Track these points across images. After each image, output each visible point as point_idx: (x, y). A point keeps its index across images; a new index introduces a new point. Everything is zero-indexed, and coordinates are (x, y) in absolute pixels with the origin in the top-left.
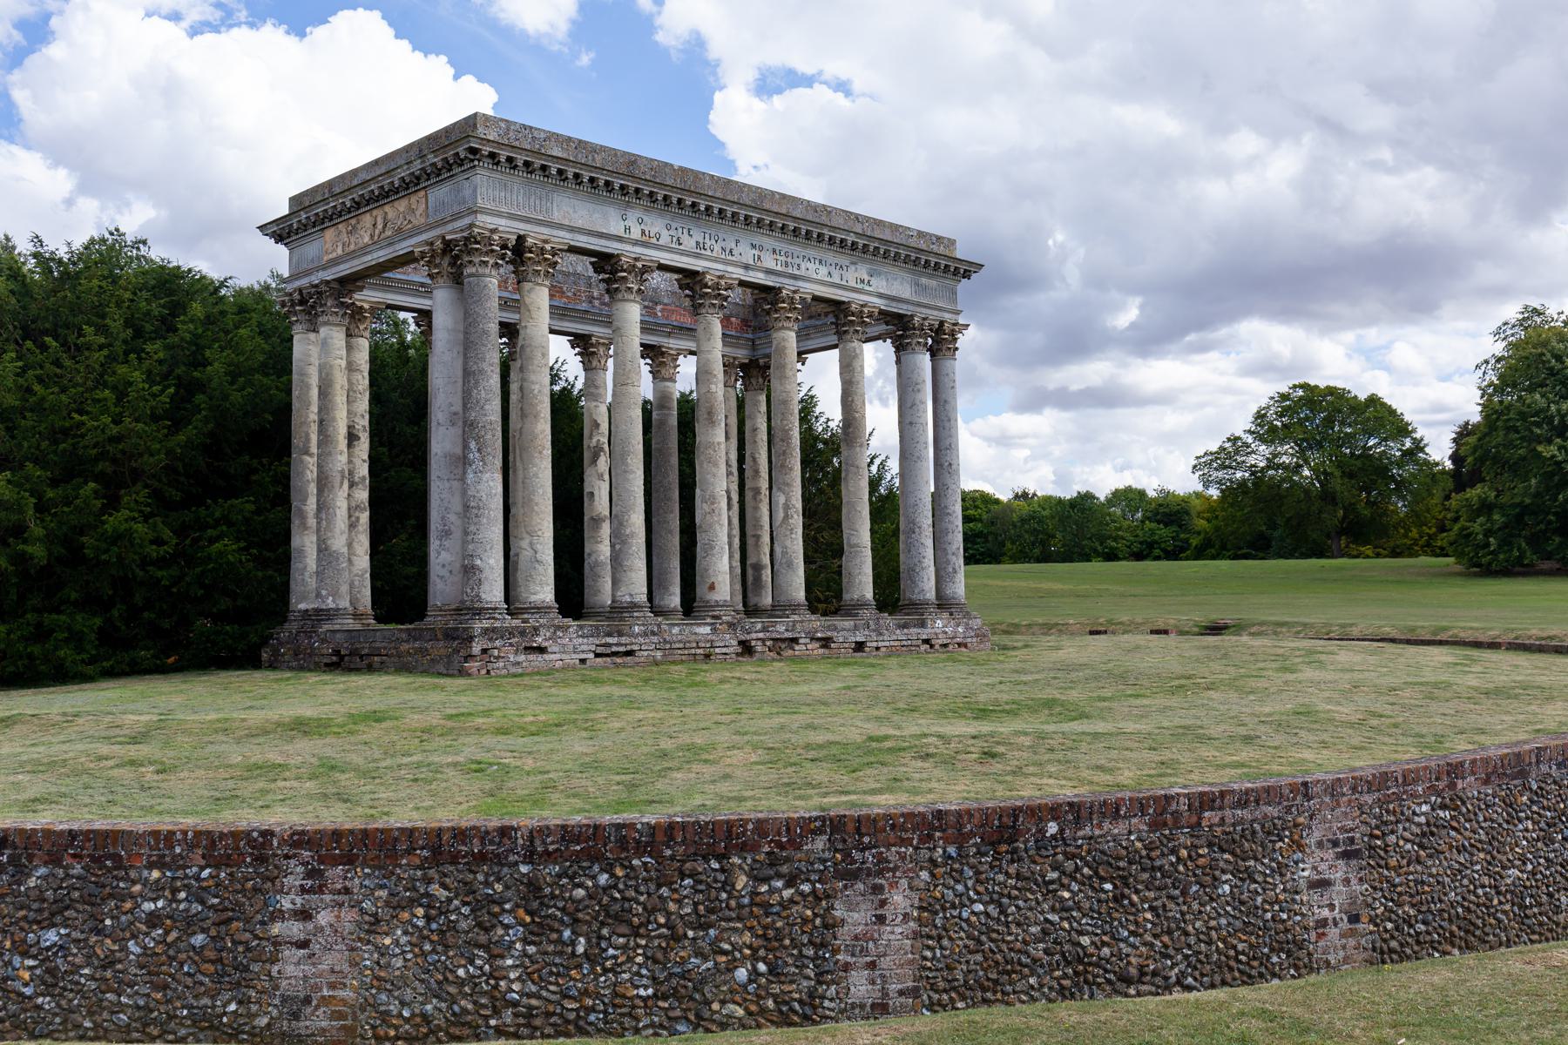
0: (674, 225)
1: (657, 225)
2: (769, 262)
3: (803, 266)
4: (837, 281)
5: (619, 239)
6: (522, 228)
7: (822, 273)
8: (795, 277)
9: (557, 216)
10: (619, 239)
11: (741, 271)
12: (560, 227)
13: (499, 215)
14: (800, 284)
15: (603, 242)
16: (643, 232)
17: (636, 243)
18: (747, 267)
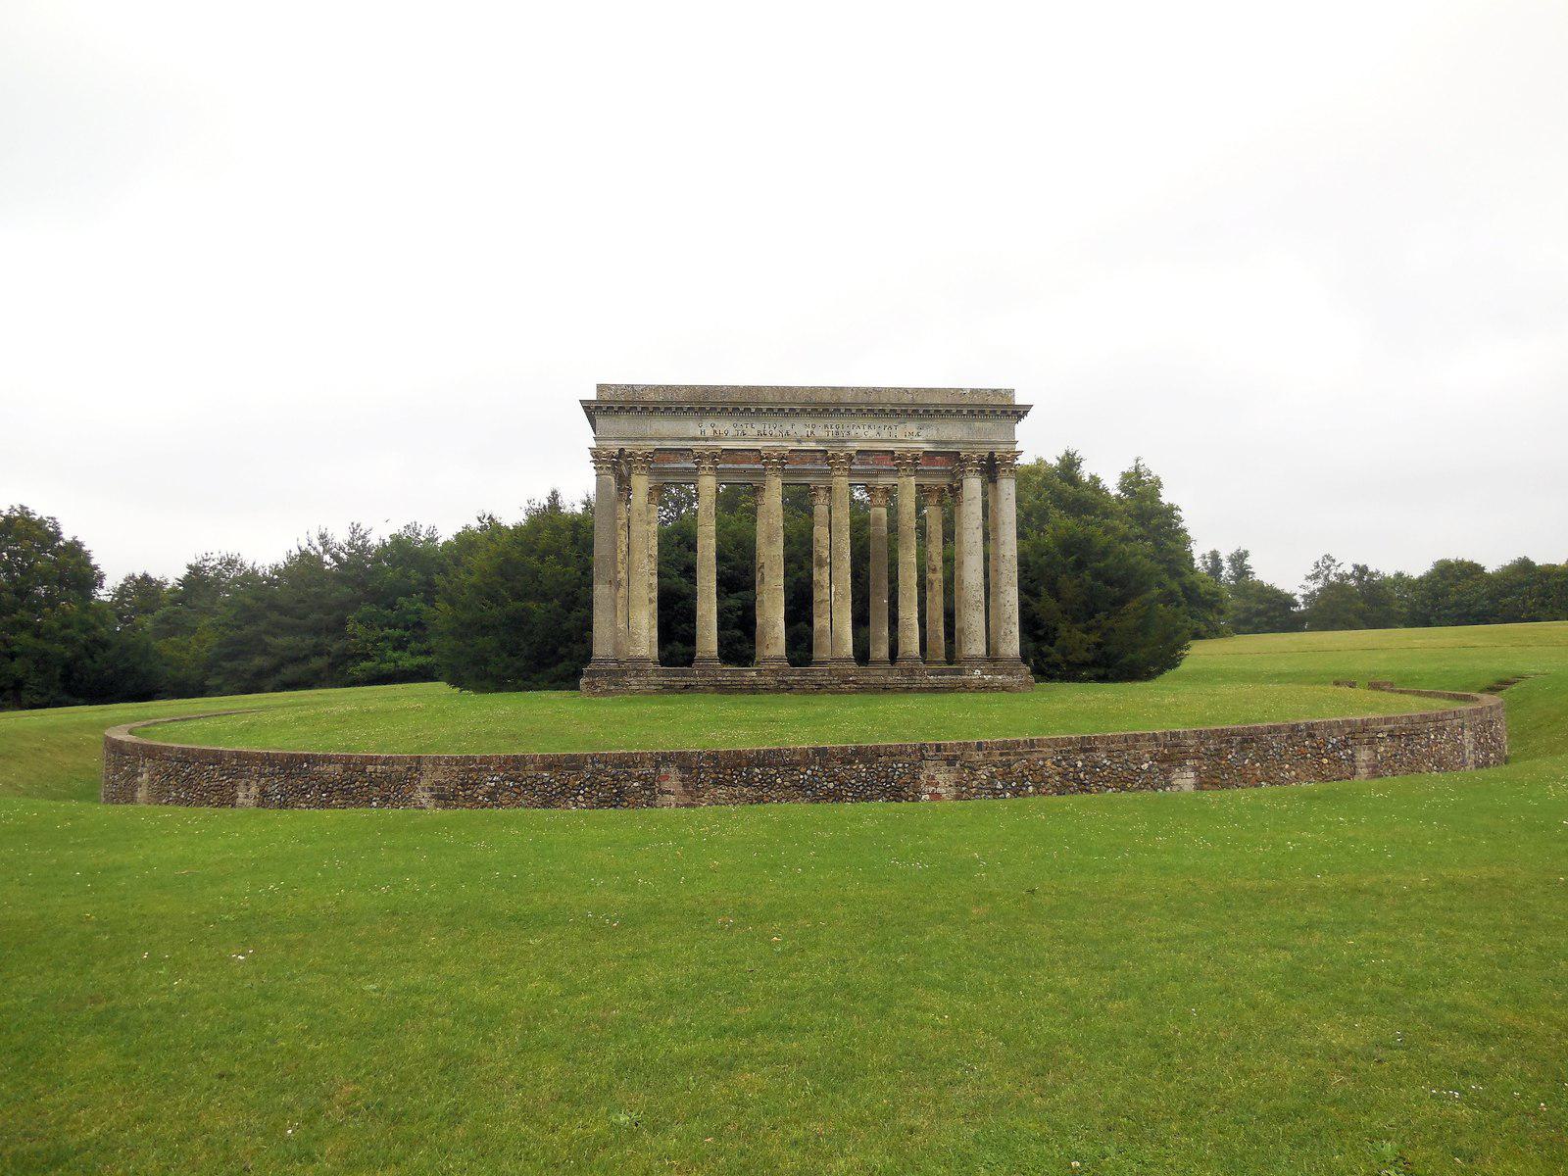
0: (739, 423)
1: (726, 426)
2: (821, 433)
3: (853, 433)
4: (885, 435)
5: (695, 439)
6: (622, 444)
7: (872, 433)
8: (844, 441)
9: (650, 432)
10: (695, 439)
11: (796, 444)
12: (651, 439)
13: (610, 439)
14: (849, 444)
15: (683, 443)
16: (715, 431)
17: (707, 439)
18: (799, 441)
